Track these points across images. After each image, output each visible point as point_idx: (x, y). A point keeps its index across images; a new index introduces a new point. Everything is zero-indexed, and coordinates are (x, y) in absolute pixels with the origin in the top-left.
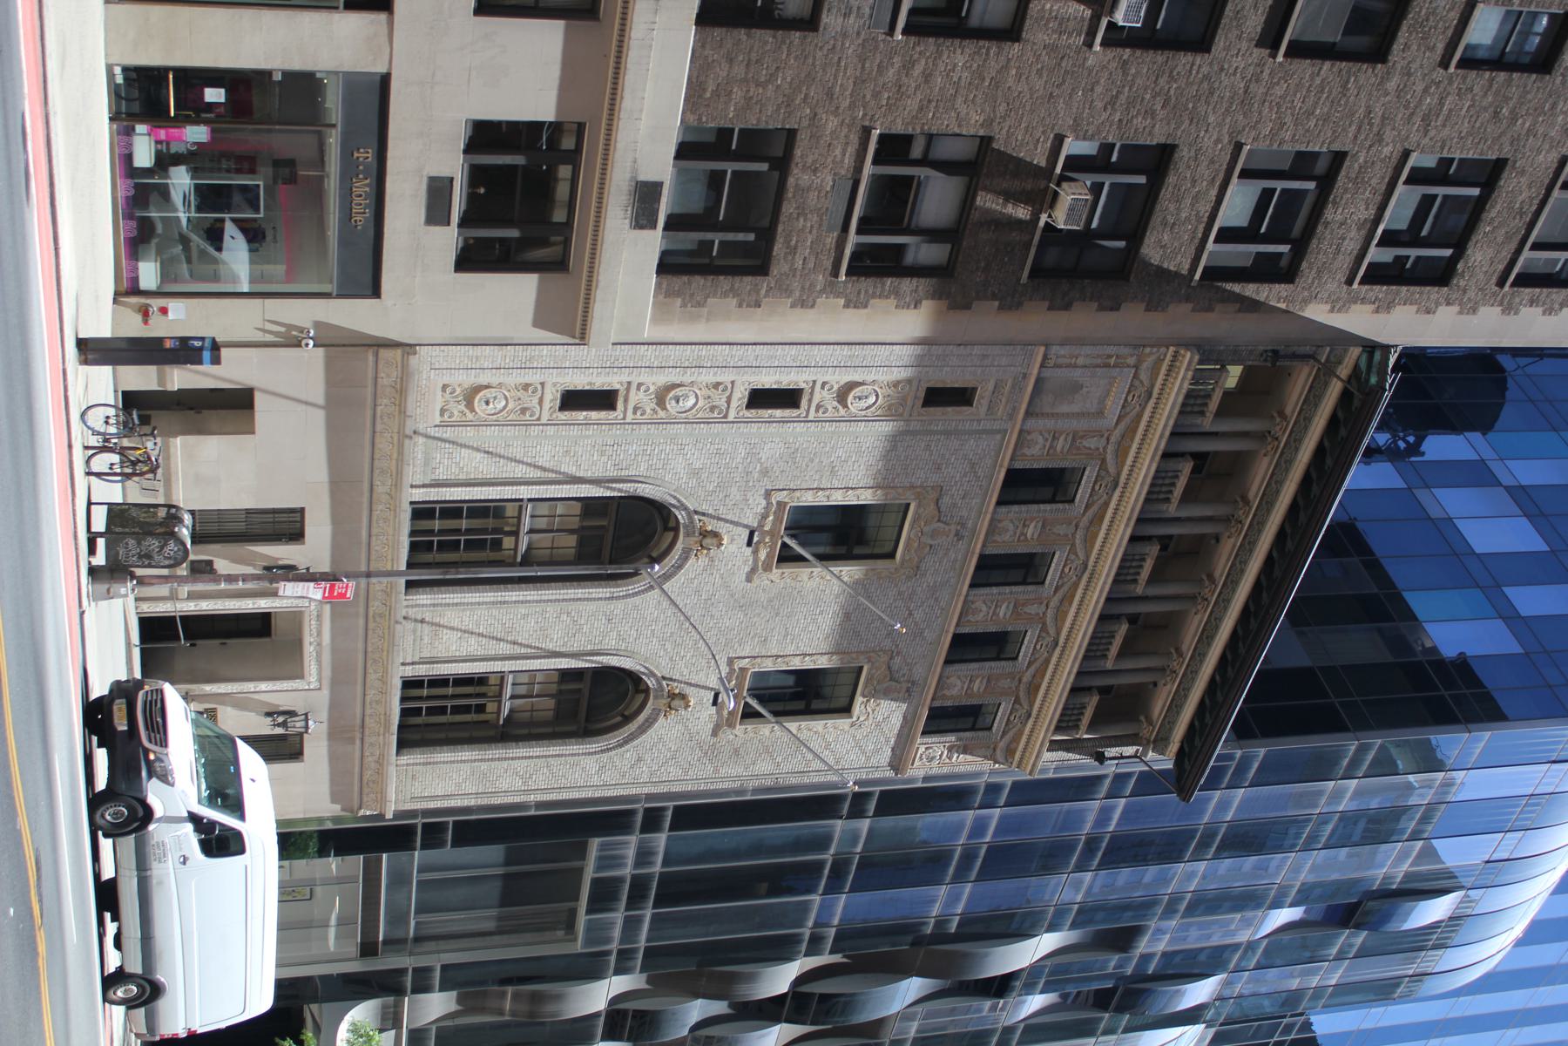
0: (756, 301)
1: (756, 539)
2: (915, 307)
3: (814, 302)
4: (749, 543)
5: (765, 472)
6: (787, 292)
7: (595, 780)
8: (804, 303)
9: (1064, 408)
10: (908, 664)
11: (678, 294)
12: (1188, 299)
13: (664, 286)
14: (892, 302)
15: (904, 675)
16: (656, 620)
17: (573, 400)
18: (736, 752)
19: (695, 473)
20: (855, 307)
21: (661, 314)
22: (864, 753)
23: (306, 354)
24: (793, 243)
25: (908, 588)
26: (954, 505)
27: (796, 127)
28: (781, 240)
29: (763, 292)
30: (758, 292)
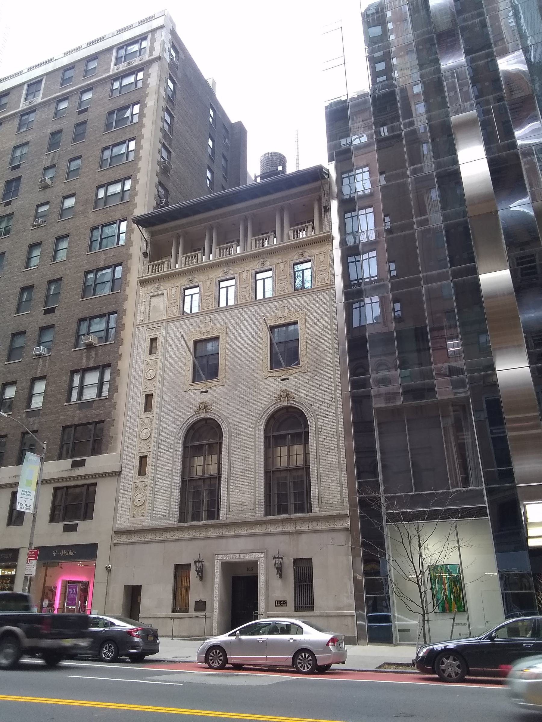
0: (112, 421)
1: (204, 390)
2: (120, 371)
3: (114, 402)
4: (207, 392)
5: (177, 396)
6: (110, 413)
7: (333, 418)
8: (114, 406)
9: (162, 308)
10: (270, 310)
11: (107, 446)
12: (125, 290)
13: (104, 451)
14: (117, 379)
15: (275, 309)
16: (240, 416)
17: (142, 471)
18: (316, 361)
19: (175, 421)
20: (118, 389)
21: (114, 450)
22: (320, 307)
23: (113, 568)
24: (95, 416)
25: (231, 326)
26: (195, 326)
27: (61, 427)
28: (93, 420)
29: (109, 420)
30: (110, 421)
